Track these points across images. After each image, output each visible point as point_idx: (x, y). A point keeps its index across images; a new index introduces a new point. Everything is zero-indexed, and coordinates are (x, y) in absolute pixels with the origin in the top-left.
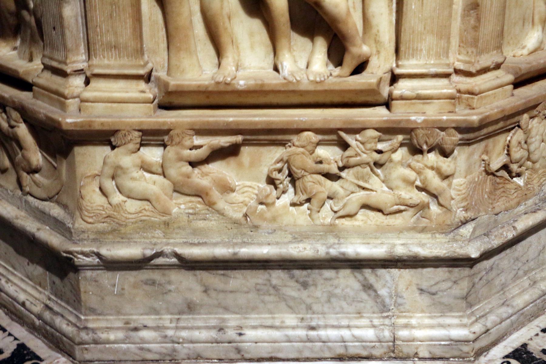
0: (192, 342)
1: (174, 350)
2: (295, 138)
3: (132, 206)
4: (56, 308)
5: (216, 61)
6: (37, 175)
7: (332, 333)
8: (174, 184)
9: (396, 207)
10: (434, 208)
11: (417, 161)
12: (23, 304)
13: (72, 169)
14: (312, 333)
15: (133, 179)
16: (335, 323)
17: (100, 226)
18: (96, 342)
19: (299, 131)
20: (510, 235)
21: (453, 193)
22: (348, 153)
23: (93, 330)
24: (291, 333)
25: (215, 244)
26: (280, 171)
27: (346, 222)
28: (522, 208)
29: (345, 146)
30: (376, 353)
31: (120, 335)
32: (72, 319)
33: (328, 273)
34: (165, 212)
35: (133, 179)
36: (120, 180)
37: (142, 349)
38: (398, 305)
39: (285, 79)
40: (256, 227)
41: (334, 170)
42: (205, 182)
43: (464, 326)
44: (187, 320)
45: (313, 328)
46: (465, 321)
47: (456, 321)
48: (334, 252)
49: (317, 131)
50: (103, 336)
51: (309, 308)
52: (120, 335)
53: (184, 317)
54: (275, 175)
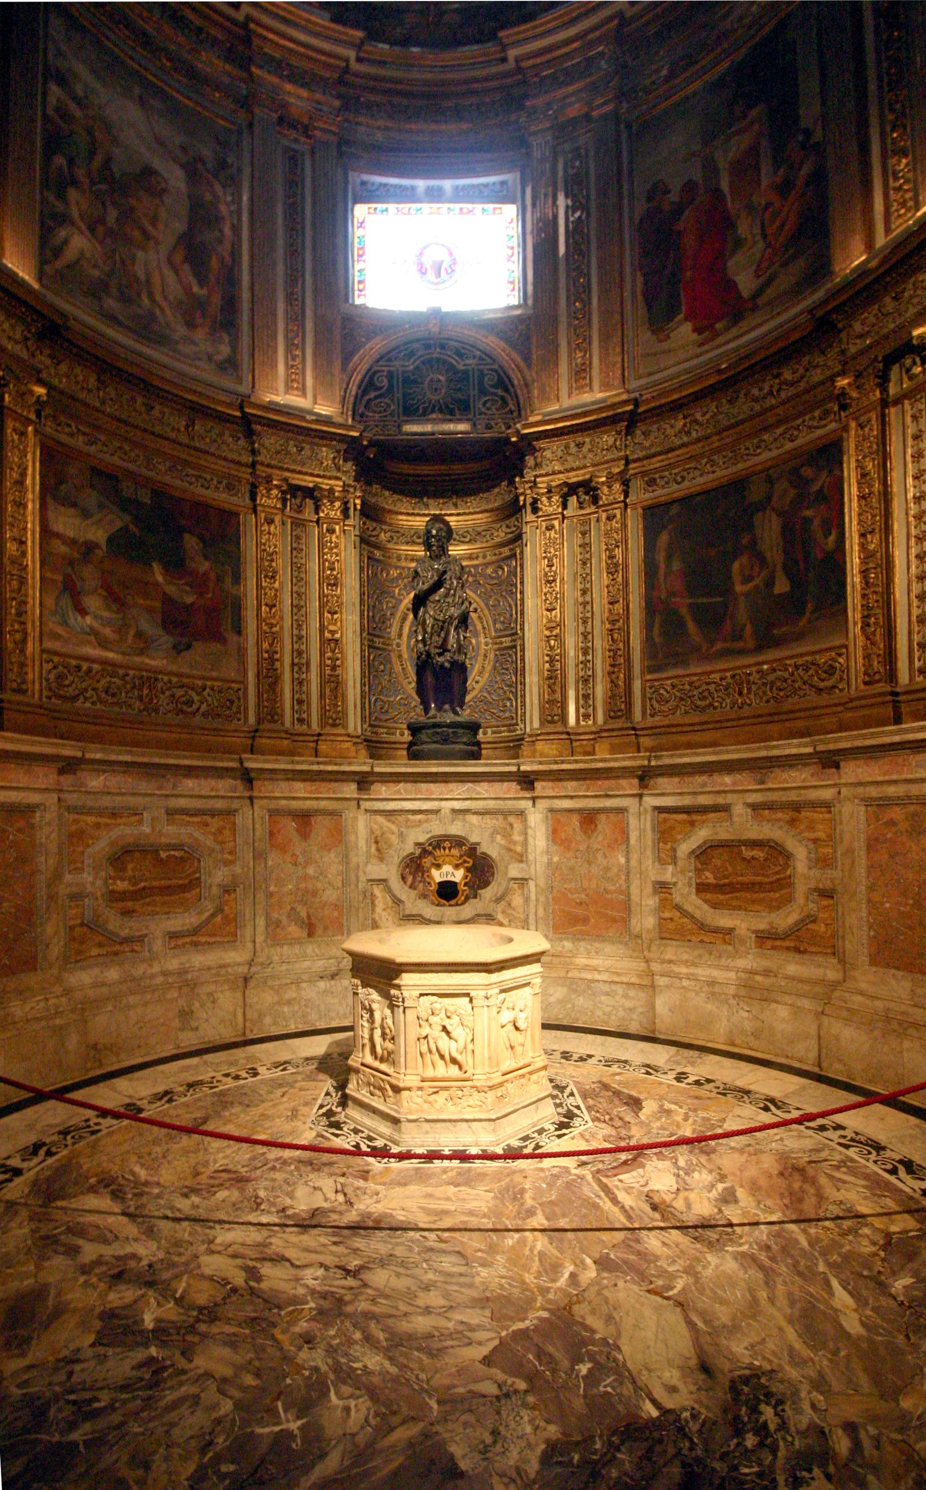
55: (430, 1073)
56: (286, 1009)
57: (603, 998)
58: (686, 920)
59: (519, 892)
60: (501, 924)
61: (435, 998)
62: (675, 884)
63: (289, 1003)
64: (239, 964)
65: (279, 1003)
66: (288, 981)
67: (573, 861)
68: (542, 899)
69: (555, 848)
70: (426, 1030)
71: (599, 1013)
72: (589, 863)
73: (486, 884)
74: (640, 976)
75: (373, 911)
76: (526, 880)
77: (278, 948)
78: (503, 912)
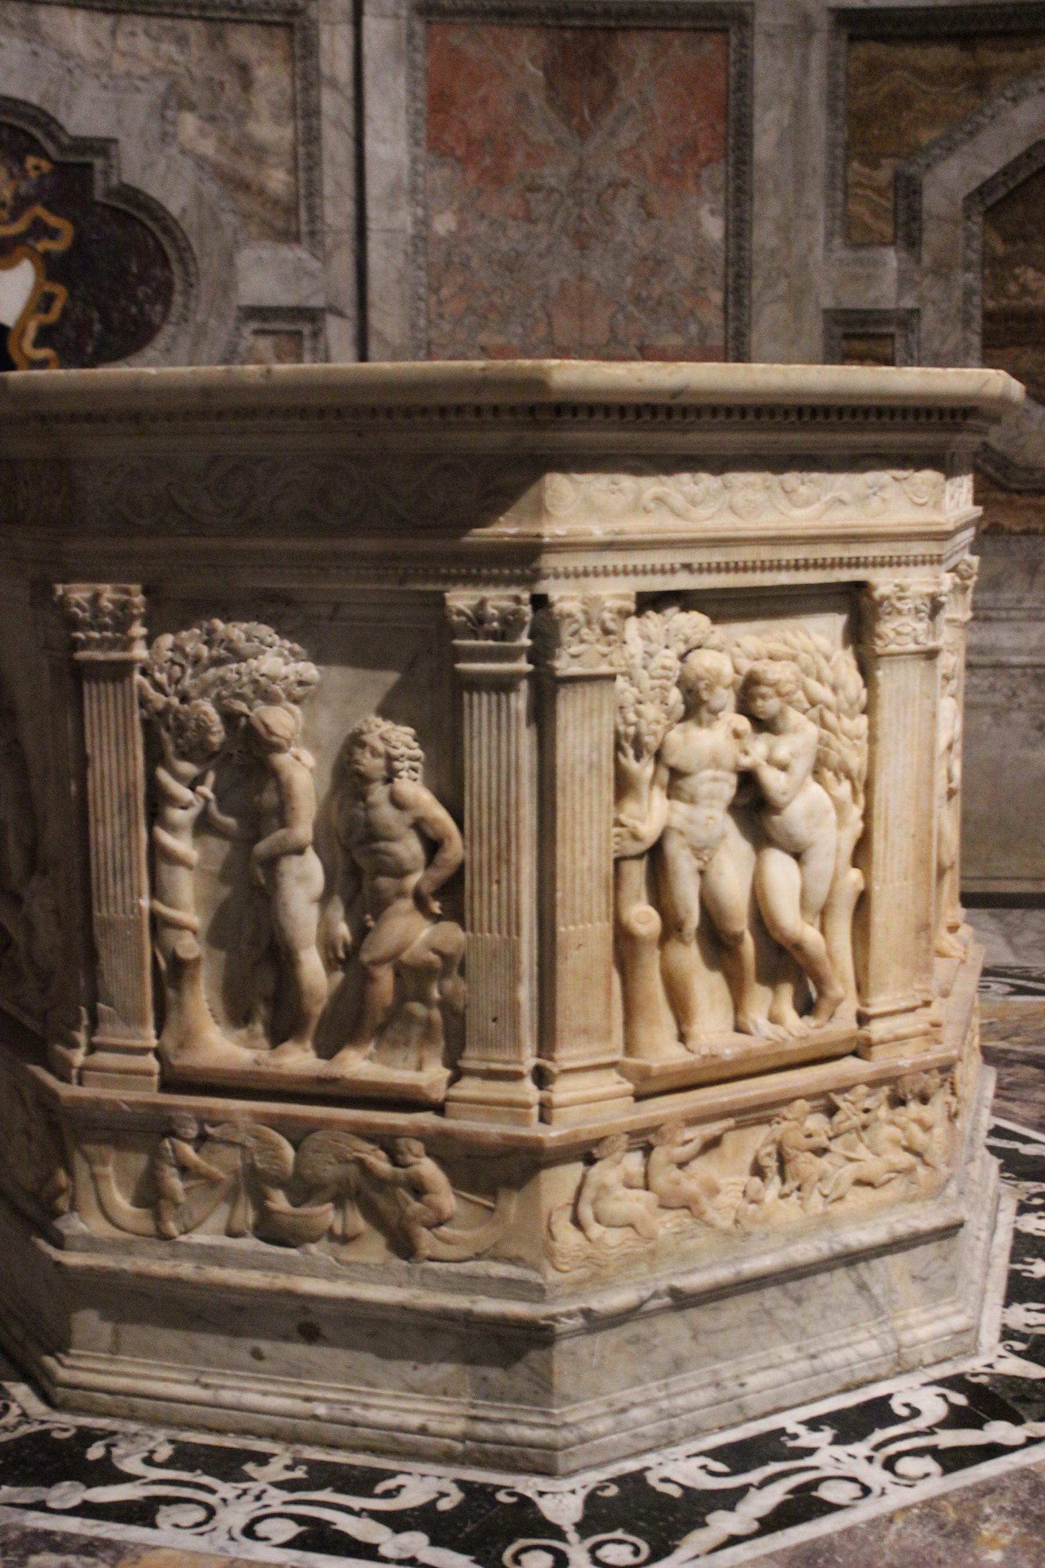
1: (672, 1428)
2: (784, 1111)
3: (614, 1237)
8: (661, 1196)
9: (887, 1176)
14: (817, 1363)
15: (617, 1199)
16: (834, 1344)
17: (577, 1274)
18: (583, 1440)
19: (789, 1101)
22: (838, 1118)
25: (710, 1267)
27: (838, 1208)
32: (541, 1420)
34: (651, 1238)
35: (617, 1199)
36: (601, 1205)
37: (635, 1436)
39: (768, 1039)
40: (748, 1234)
41: (825, 1143)
45: (813, 1357)
49: (809, 1098)
50: (590, 1429)
51: (803, 1330)
53: (672, 1379)
67: (515, 232)
69: (440, 176)
72: (582, 240)
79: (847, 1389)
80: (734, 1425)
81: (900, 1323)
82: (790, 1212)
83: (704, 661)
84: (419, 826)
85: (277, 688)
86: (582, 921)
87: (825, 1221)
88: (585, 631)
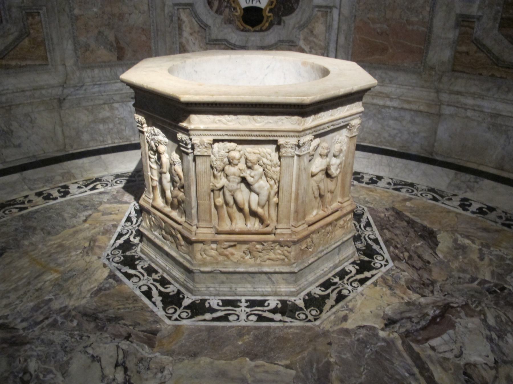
0: (223, 291)
1: (219, 293)
3: (208, 258)
4: (187, 281)
5: (230, 222)
6: (183, 247)
7: (260, 290)
10: (286, 260)
11: (281, 248)
12: (178, 278)
13: (193, 248)
14: (255, 290)
20: (307, 265)
21: (291, 256)
23: (198, 288)
24: (249, 289)
25: (230, 268)
26: (247, 251)
27: (264, 263)
28: (311, 256)
29: (263, 245)
30: (271, 294)
31: (205, 289)
33: (259, 275)
38: (277, 283)
41: (260, 250)
42: (227, 253)
43: (294, 288)
44: (222, 286)
45: (255, 288)
46: (294, 286)
47: (292, 287)
48: (260, 270)
52: (205, 289)
54: (246, 252)
55: (226, 226)
56: (101, 126)
57: (391, 122)
58: (481, 54)
59: (322, 20)
60: (302, 51)
61: (233, 145)
62: (479, 18)
63: (104, 121)
64: (53, 87)
65: (94, 122)
66: (101, 102)
68: (344, 27)
70: (222, 181)
71: (386, 135)
73: (290, 11)
74: (429, 105)
75: (181, 35)
76: (331, 8)
77: (89, 72)
78: (305, 39)
79: (262, 296)
80: (233, 296)
81: (278, 287)
82: (252, 261)
83: (235, 154)
84: (178, 175)
85: (162, 142)
86: (204, 200)
87: (260, 265)
88: (201, 147)
